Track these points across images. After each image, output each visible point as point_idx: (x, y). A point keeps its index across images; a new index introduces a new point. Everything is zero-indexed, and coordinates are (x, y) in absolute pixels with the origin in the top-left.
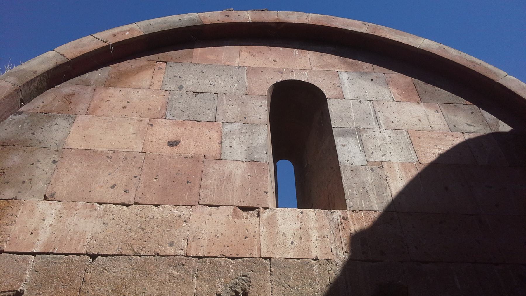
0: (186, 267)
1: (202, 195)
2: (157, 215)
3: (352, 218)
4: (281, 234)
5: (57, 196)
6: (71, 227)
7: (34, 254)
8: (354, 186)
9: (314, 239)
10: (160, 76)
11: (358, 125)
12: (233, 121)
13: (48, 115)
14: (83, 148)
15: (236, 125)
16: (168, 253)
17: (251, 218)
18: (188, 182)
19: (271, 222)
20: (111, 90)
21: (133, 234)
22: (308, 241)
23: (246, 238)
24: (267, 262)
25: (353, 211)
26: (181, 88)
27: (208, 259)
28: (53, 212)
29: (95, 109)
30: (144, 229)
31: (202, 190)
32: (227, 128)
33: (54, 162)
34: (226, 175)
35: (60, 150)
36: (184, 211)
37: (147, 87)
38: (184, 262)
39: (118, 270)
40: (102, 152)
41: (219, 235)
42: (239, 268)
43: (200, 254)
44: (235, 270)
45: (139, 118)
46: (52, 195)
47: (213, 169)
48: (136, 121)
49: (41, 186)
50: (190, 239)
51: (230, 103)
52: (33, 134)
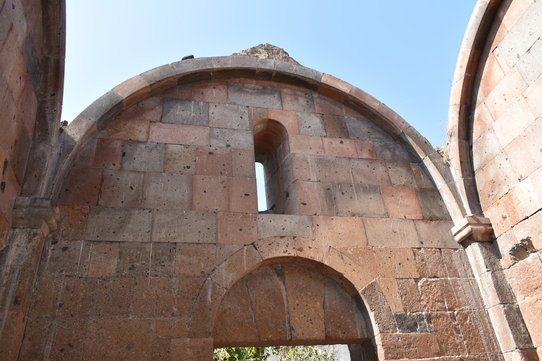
5: (523, 175)
14: (510, 141)
20: (491, 95)
26: (518, 56)
29: (495, 113)
33: (507, 159)
35: (503, 151)
37: (503, 75)
40: (520, 136)
45: (517, 99)
46: (521, 177)
49: (513, 177)
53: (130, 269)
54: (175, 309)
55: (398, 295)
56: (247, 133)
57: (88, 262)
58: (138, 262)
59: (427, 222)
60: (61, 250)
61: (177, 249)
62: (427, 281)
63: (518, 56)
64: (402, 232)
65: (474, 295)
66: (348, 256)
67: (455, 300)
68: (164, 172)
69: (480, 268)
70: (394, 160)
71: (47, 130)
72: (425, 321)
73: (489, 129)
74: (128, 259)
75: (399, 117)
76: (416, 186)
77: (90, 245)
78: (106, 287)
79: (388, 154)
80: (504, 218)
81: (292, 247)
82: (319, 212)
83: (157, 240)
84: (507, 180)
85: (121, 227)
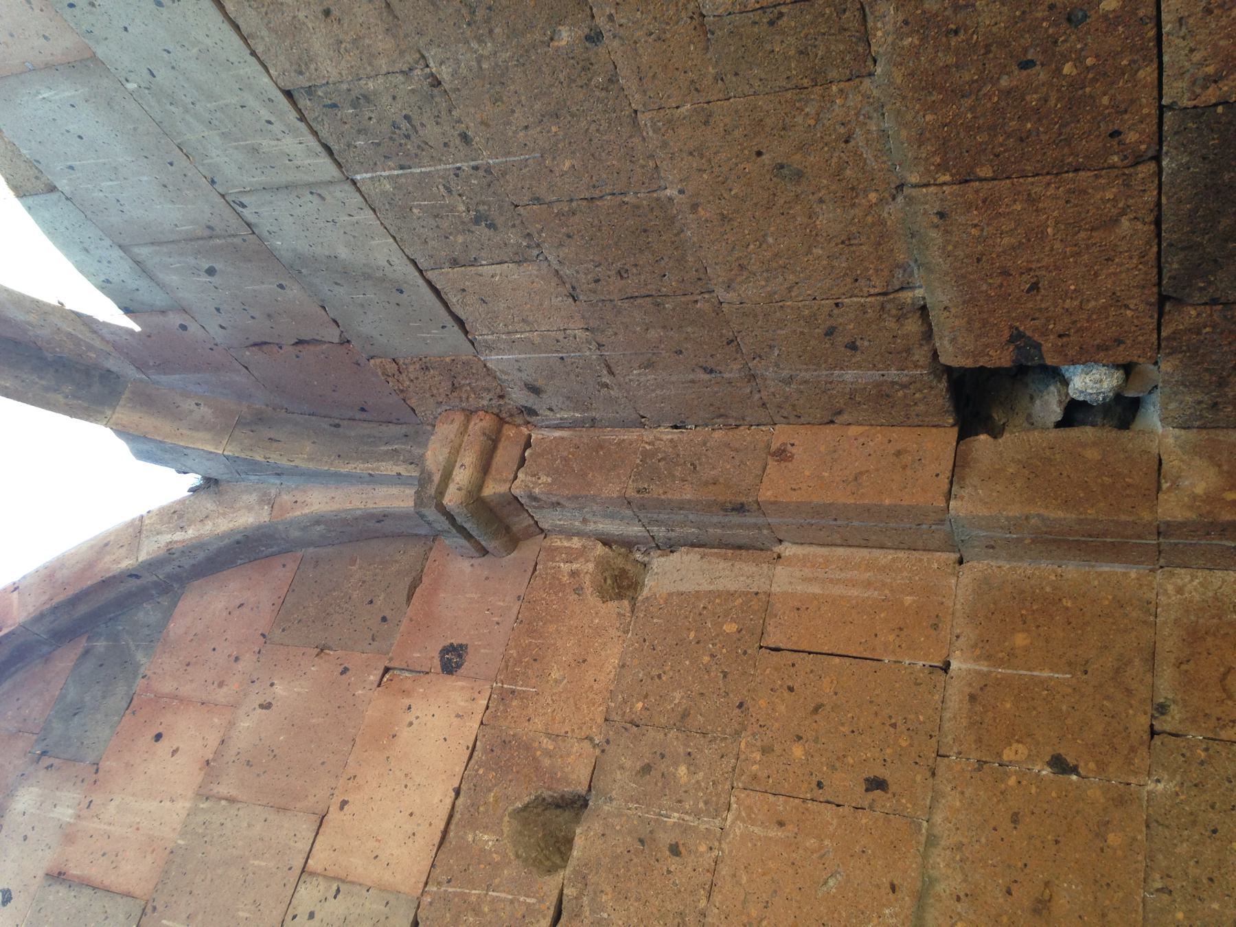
53: (492, 226)
54: (566, 36)
57: (543, 337)
58: (452, 209)
60: (544, 396)
61: (302, 81)
68: (52, 189)
71: (238, 543)
74: (460, 239)
77: (486, 341)
78: (597, 281)
83: (325, 160)
85: (367, 277)
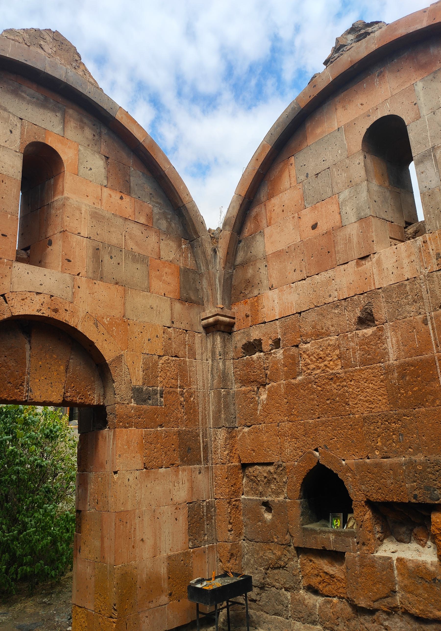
0: (340, 306)
1: (338, 258)
2: (319, 281)
3: (430, 239)
4: (385, 270)
5: (274, 286)
6: (286, 301)
7: (277, 320)
8: (431, 210)
9: (405, 266)
10: (293, 172)
11: (433, 143)
12: (344, 188)
13: (253, 235)
15: (346, 191)
16: (330, 301)
17: (367, 264)
18: (329, 252)
19: (379, 262)
21: (311, 296)
22: (402, 268)
23: (366, 279)
24: (380, 290)
25: (431, 233)
26: (307, 176)
27: (349, 299)
28: (276, 296)
30: (315, 291)
31: (337, 255)
32: (342, 197)
34: (348, 238)
35: (265, 258)
36: (331, 273)
37: (289, 186)
38: (338, 304)
39: (312, 317)
40: (283, 250)
41: (352, 282)
42: (366, 299)
43: (345, 297)
44: (363, 301)
46: (272, 287)
47: (340, 235)
48: (292, 219)
49: (265, 282)
50: (338, 290)
51: (339, 173)
52: (251, 252)
55: (141, 370)
56: (16, 156)
59: (182, 303)
62: (169, 359)
63: (307, 176)
64: (158, 309)
65: (203, 377)
66: (103, 324)
67: (187, 379)
69: (215, 354)
70: (167, 233)
72: (158, 395)
73: (260, 232)
75: (185, 187)
76: (181, 265)
79: (164, 224)
80: (247, 316)
81: (47, 307)
82: (83, 273)
84: (260, 284)
